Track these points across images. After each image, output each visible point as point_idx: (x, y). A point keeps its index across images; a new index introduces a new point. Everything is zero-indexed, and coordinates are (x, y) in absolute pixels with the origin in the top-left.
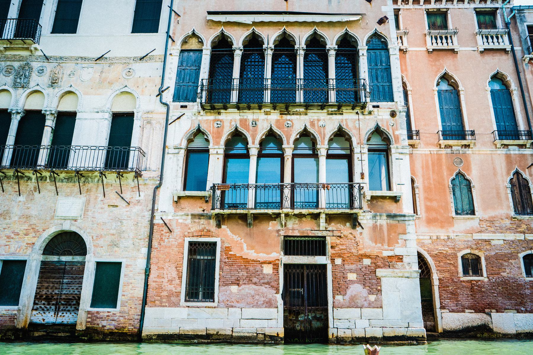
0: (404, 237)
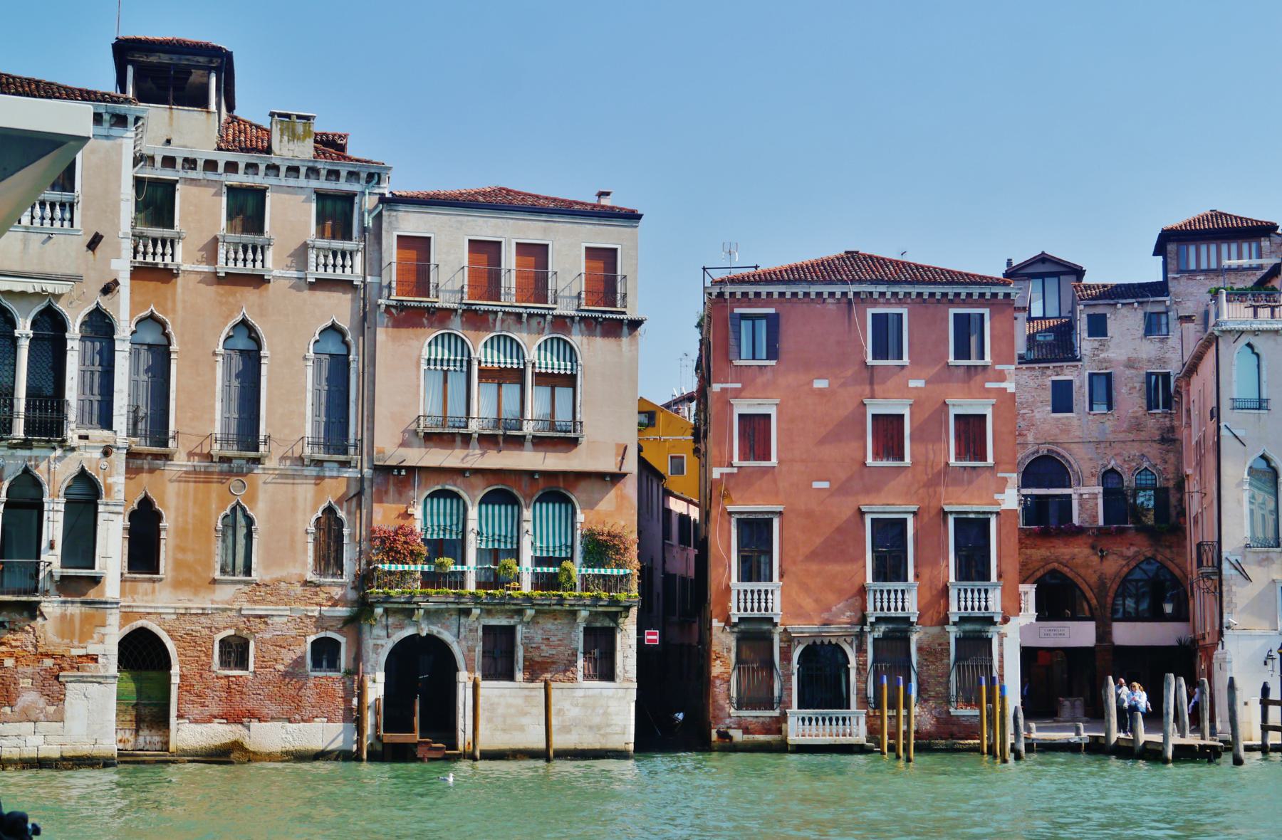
0: (102, 630)
